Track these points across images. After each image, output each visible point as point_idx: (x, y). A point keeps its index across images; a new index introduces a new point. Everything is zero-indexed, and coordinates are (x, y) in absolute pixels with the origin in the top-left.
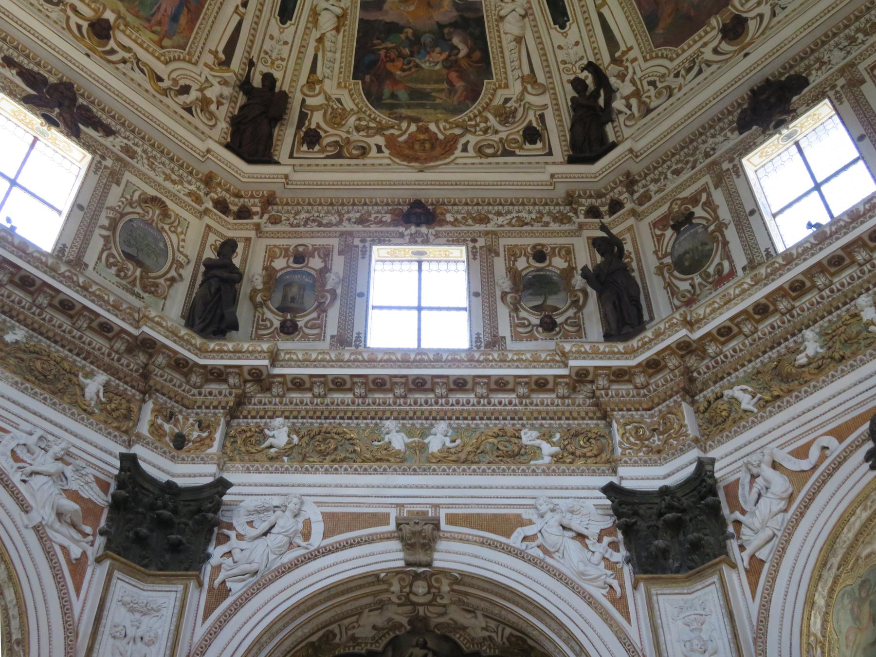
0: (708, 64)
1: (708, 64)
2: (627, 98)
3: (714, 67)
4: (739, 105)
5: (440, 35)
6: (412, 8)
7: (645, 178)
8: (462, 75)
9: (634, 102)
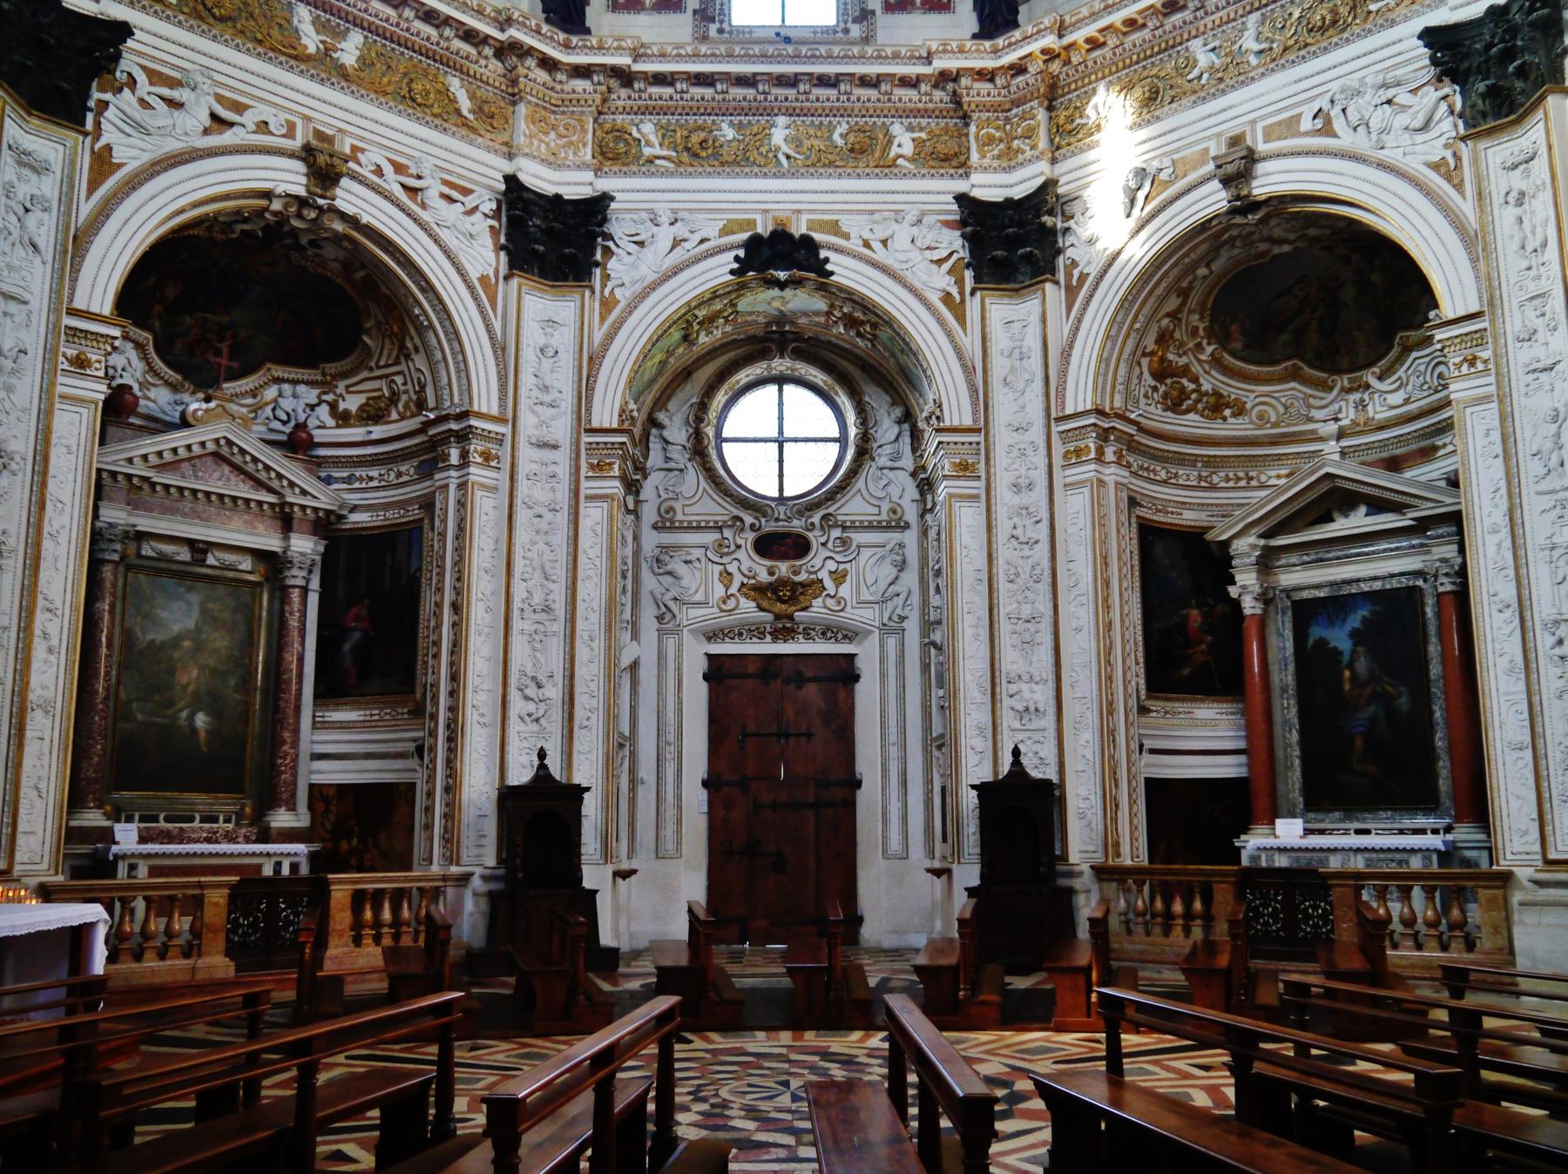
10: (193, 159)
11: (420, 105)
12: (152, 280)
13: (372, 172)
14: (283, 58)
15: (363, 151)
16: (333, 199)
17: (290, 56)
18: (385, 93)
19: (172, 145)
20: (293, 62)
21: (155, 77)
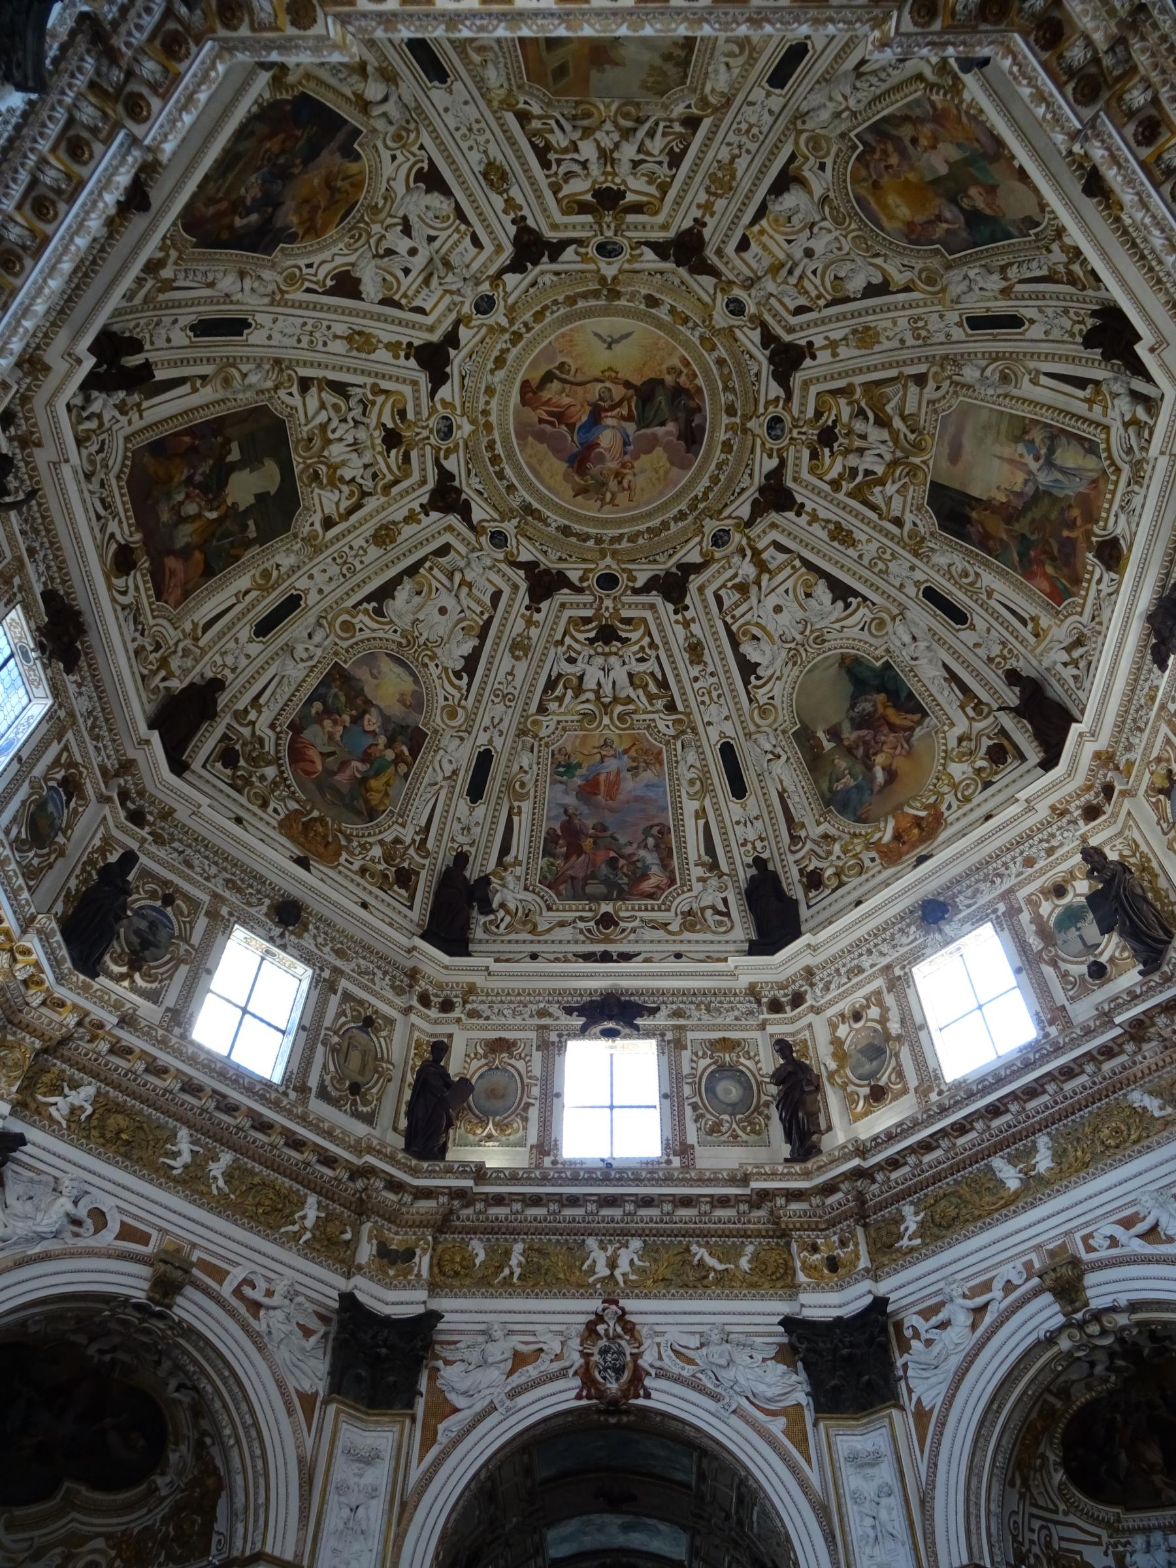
0: (103, 529)
1: (103, 529)
2: (99, 416)
3: (98, 536)
4: (68, 594)
5: (270, 202)
6: (316, 181)
7: (23, 460)
8: (219, 215)
9: (93, 424)
10: (972, 1362)
11: (1117, 1147)
12: (1123, 1457)
13: (1109, 1248)
14: (996, 1216)
15: (1090, 1235)
16: (1087, 1304)
17: (1003, 1207)
18: (1086, 1165)
19: (955, 1361)
20: (1004, 1211)
21: (926, 1314)
